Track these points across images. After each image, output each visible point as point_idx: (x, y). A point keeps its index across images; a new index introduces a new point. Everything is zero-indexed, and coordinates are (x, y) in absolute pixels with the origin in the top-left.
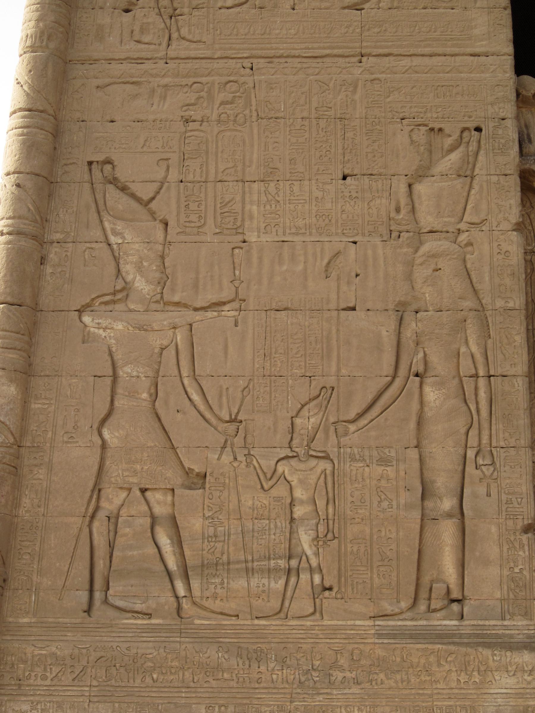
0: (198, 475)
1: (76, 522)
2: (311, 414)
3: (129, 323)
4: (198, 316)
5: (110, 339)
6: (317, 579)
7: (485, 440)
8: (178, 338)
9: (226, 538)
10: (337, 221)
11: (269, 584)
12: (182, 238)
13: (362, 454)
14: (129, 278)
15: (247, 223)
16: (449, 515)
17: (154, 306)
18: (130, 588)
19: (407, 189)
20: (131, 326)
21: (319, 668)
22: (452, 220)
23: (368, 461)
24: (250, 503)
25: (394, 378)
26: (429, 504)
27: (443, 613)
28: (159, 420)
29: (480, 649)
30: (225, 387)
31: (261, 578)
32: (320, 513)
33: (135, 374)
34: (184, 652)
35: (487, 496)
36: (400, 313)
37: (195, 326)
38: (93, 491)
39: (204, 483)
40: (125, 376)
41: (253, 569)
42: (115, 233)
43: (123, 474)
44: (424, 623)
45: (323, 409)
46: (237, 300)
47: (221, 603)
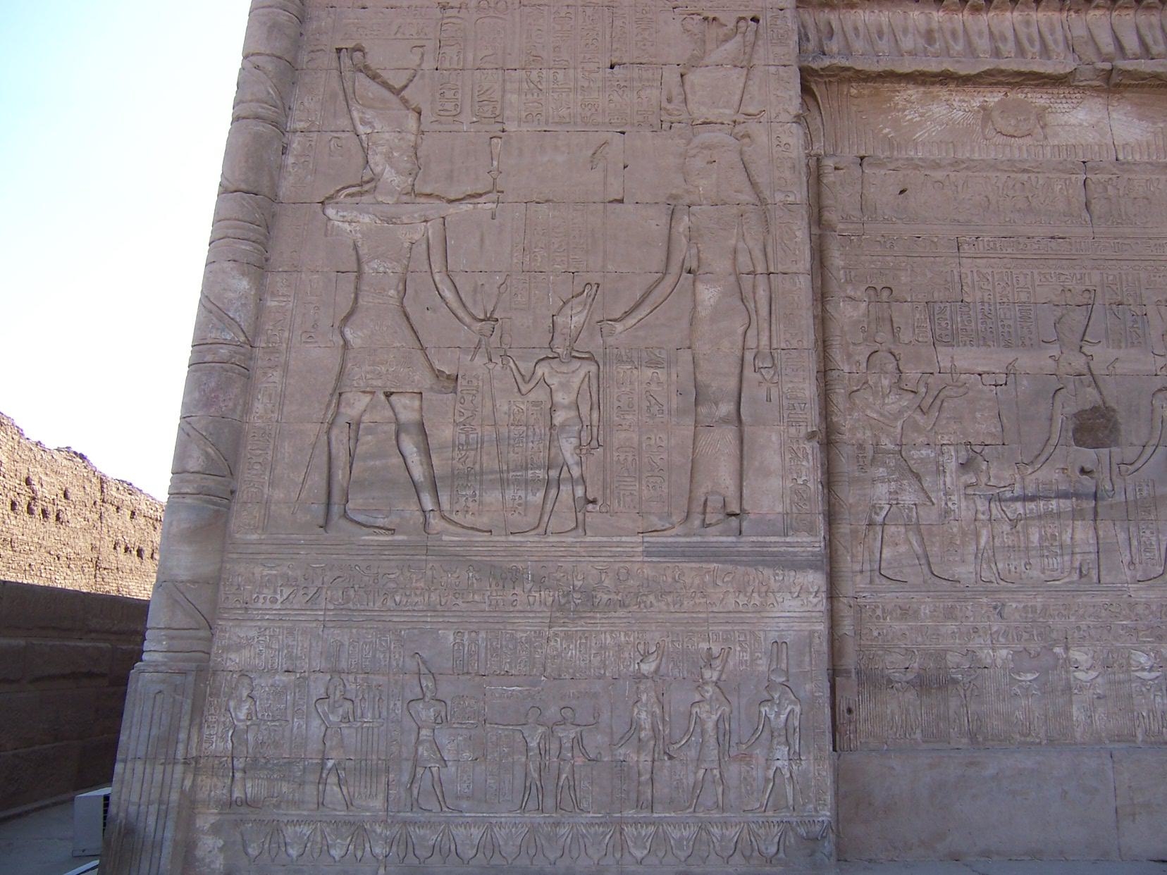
0: (448, 377)
1: (312, 429)
2: (574, 312)
4: (452, 210)
5: (356, 233)
6: (580, 492)
7: (764, 341)
8: (430, 232)
9: (479, 446)
10: (604, 111)
11: (526, 497)
12: (436, 127)
13: (629, 355)
14: (378, 170)
15: (507, 113)
16: (725, 421)
17: (405, 198)
18: (371, 501)
19: (679, 79)
20: (379, 219)
21: (582, 590)
22: (727, 111)
23: (636, 363)
24: (505, 408)
25: (665, 273)
26: (703, 410)
27: (720, 527)
28: (408, 318)
31: (518, 490)
32: (584, 419)
33: (381, 269)
34: (430, 573)
36: (672, 207)
37: (448, 219)
38: (332, 395)
39: (455, 387)
40: (371, 271)
41: (508, 480)
42: (363, 122)
44: (699, 539)
45: (588, 307)
46: (495, 192)
47: (473, 518)
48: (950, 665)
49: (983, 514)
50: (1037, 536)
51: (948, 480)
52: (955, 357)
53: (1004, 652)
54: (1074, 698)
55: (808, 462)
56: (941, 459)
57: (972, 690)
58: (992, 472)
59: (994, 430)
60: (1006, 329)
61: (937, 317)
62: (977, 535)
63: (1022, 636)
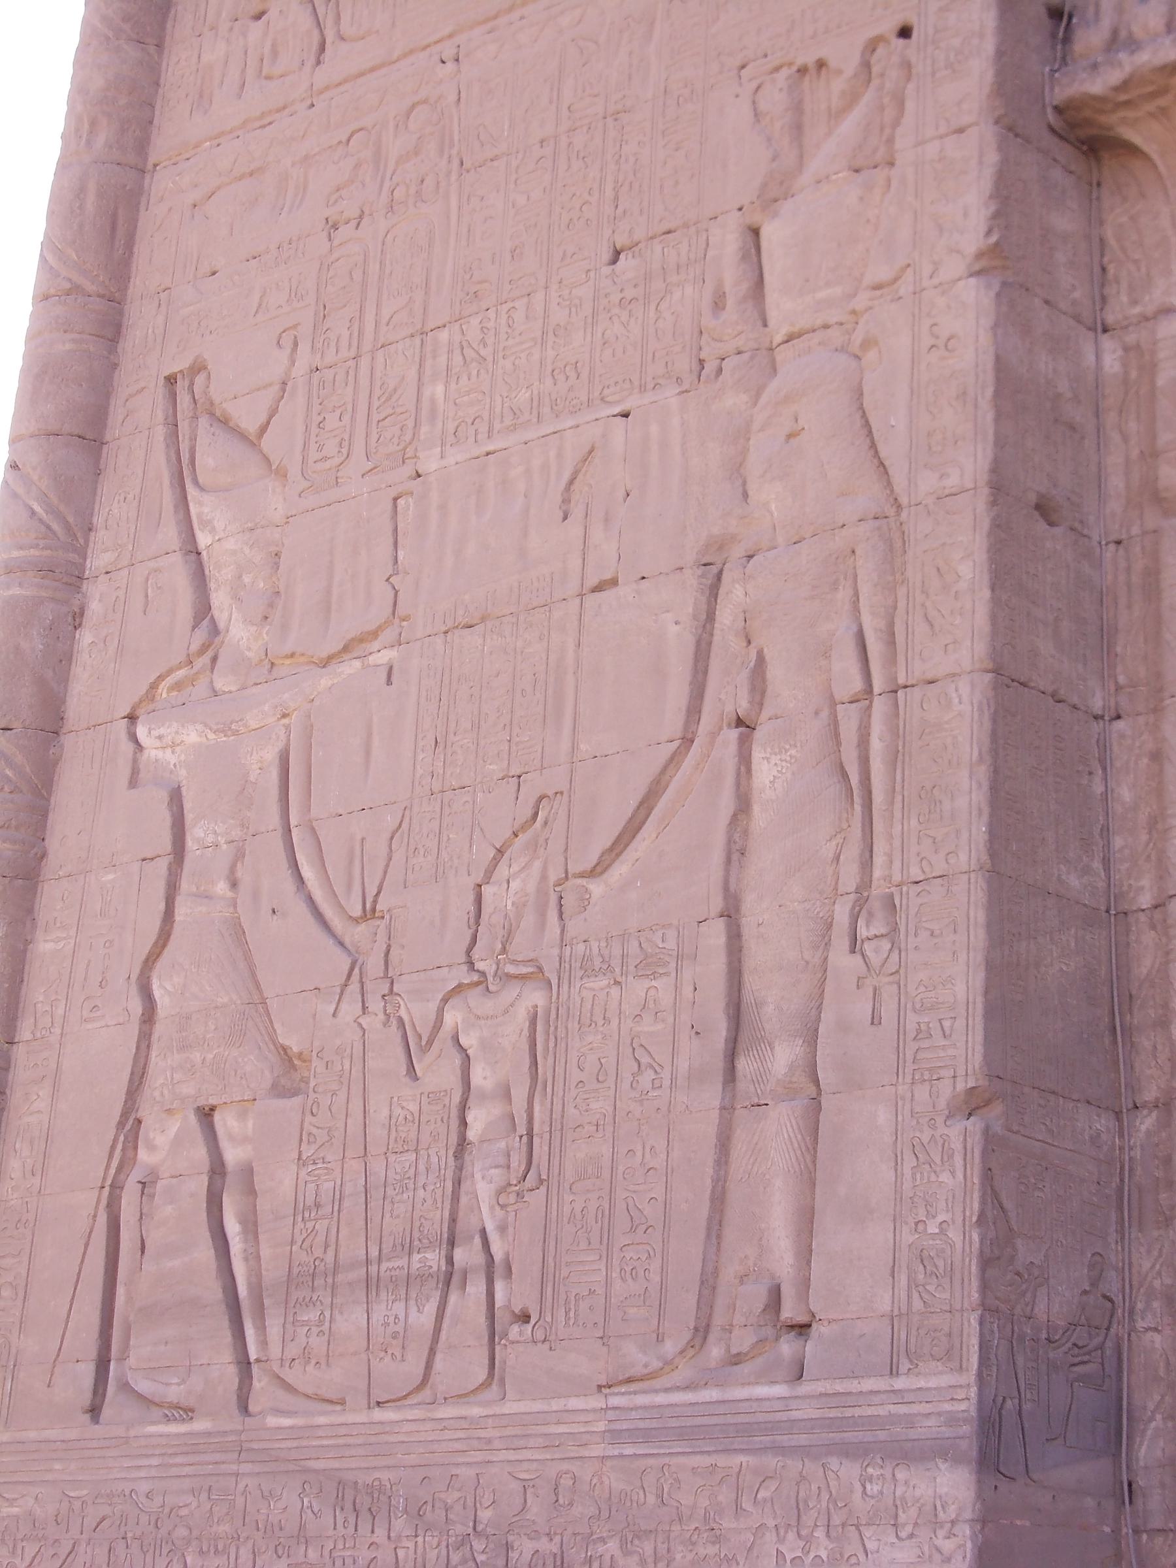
2: (515, 868)
3: (206, 725)
13: (606, 952)
22: (837, 291)
23: (618, 970)
25: (688, 741)
29: (834, 1462)
30: (359, 837)
33: (210, 839)
35: (872, 1023)
36: (714, 569)
43: (172, 1079)
46: (397, 621)
55: (953, 1173)
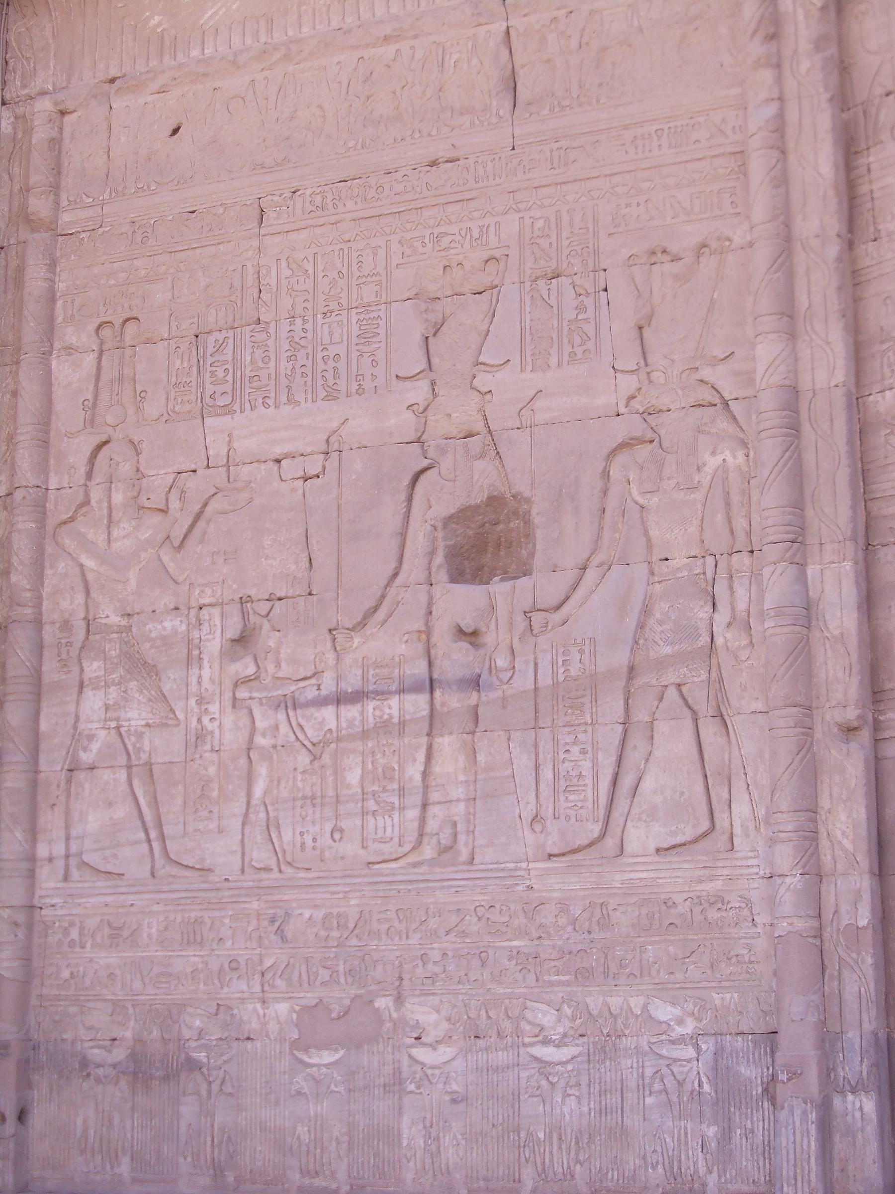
48: (187, 1034)
49: (264, 735)
50: (358, 772)
51: (206, 673)
52: (235, 433)
53: (283, 1008)
54: (407, 1099)
56: (195, 634)
57: (223, 1081)
58: (284, 653)
59: (293, 567)
60: (331, 363)
61: (209, 360)
62: (250, 778)
63: (317, 974)
